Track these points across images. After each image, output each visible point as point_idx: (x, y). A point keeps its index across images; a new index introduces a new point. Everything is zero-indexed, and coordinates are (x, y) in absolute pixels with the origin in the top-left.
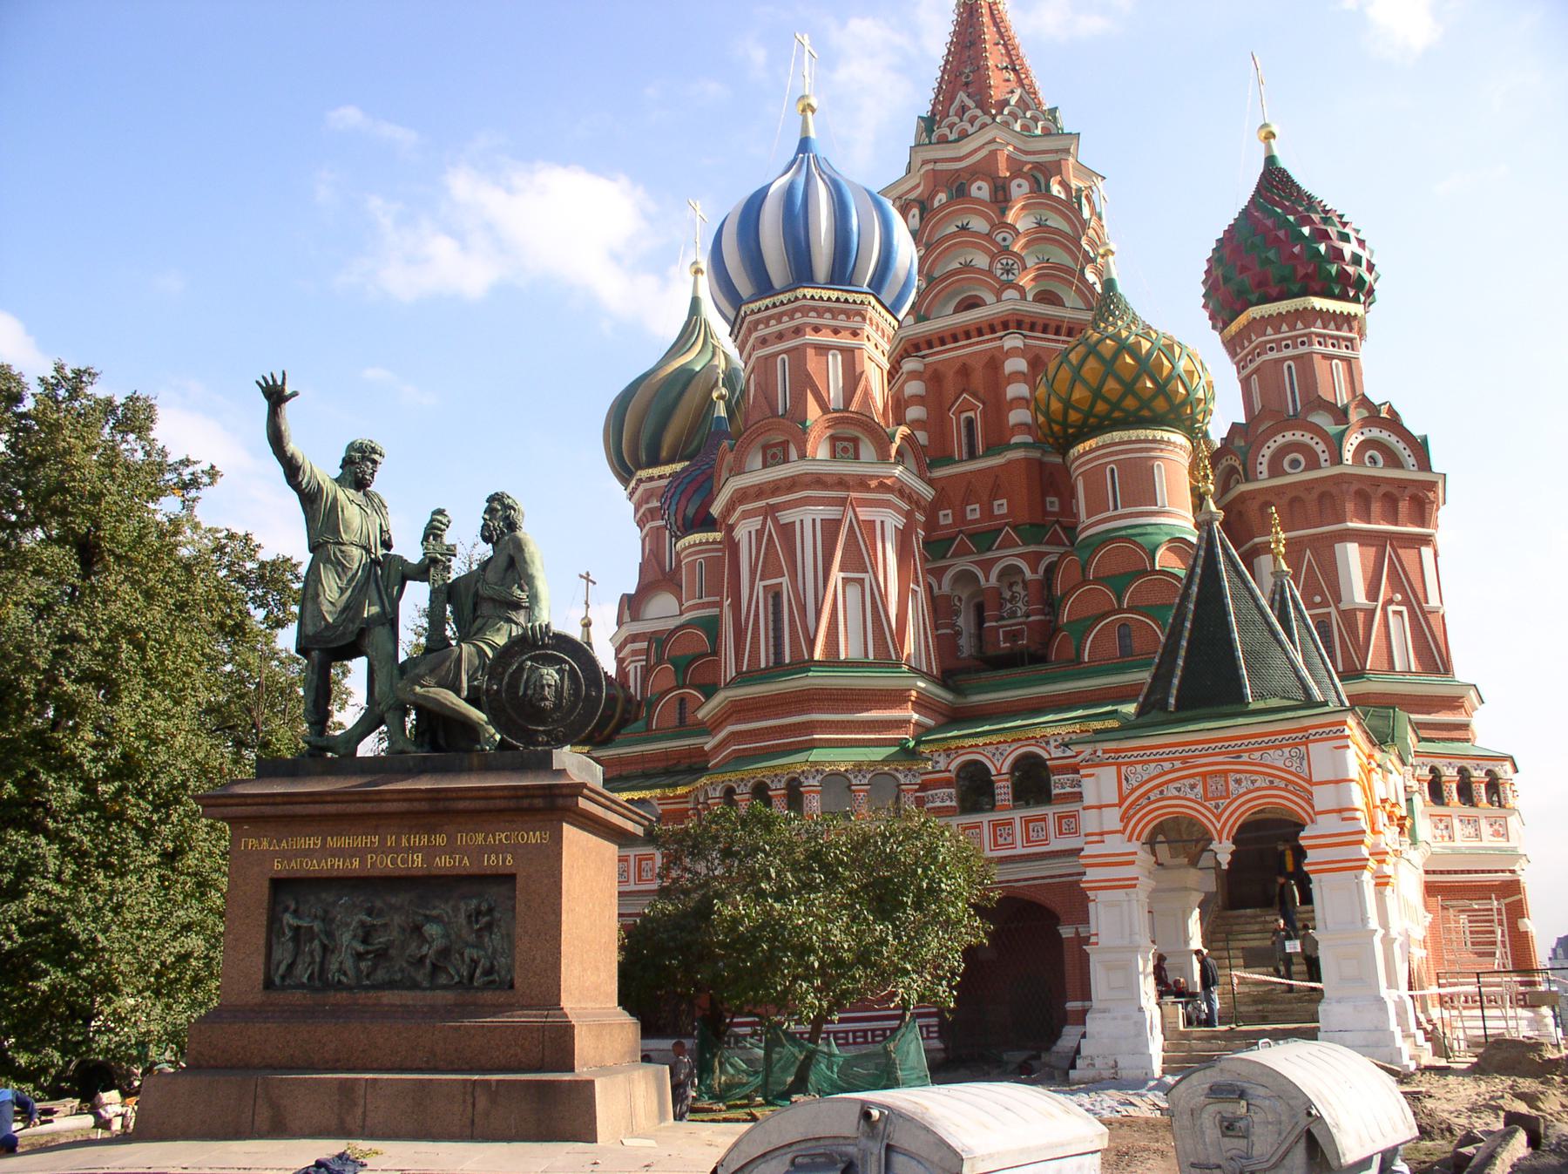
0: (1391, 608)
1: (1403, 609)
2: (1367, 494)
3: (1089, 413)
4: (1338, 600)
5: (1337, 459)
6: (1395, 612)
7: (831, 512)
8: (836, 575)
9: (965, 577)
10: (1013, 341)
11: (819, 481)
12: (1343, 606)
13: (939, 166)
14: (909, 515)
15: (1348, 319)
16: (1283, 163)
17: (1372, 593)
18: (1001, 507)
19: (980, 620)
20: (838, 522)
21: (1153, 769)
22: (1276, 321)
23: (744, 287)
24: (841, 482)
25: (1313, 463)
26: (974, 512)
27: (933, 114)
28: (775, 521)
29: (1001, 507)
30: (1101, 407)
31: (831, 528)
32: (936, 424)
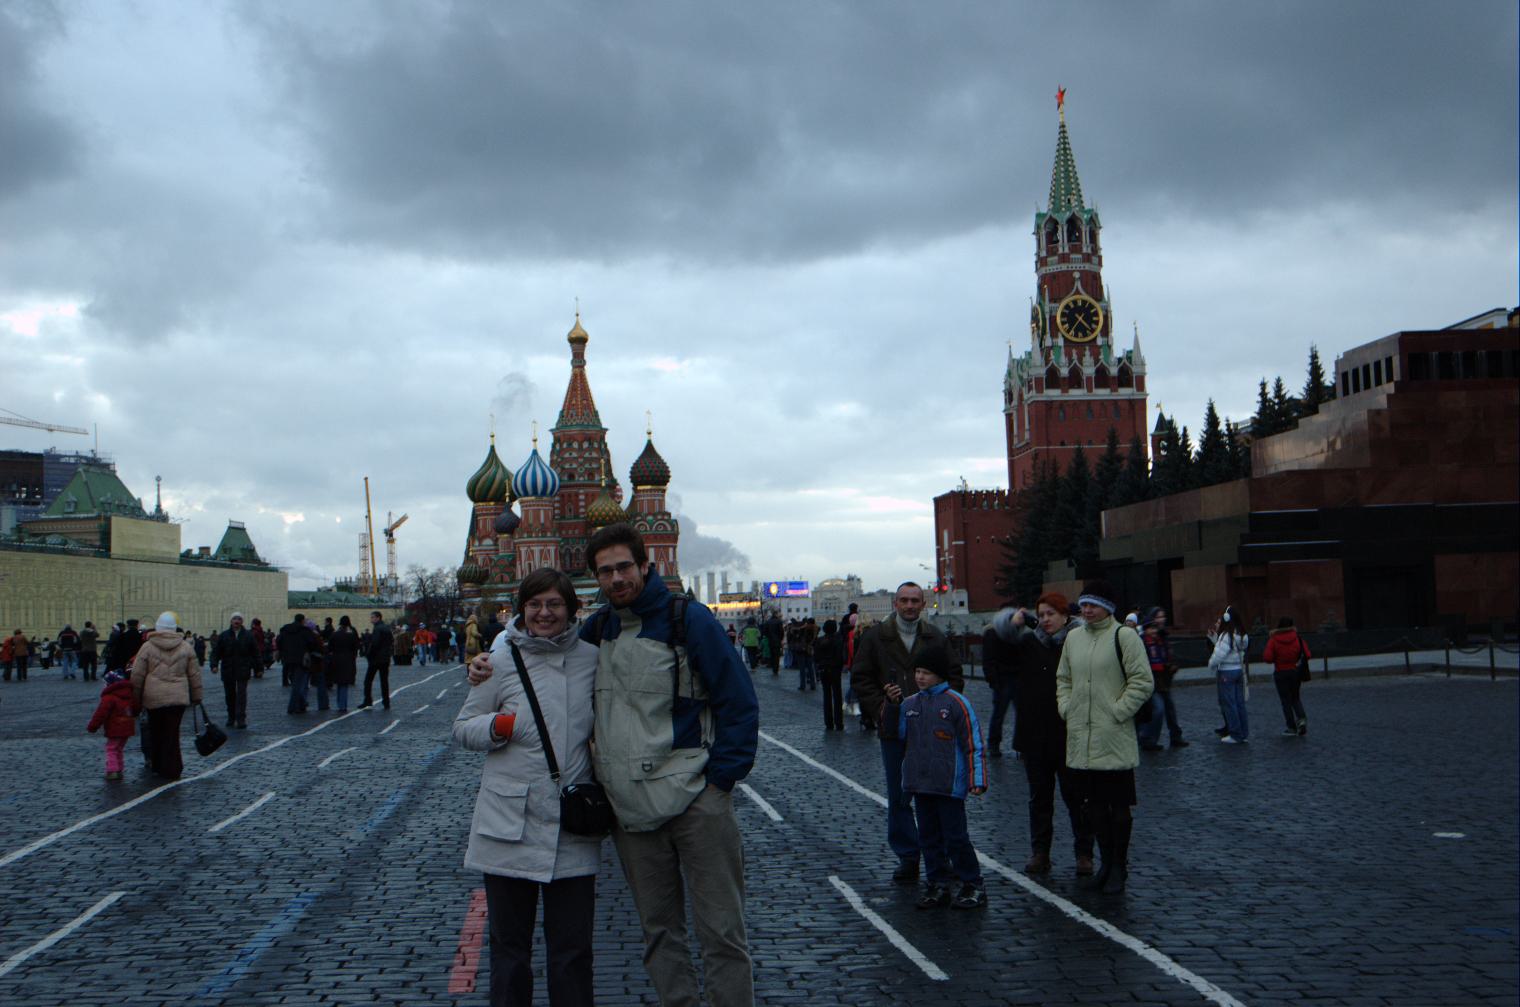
2: (657, 537)
5: (651, 528)
9: (567, 549)
10: (581, 491)
11: (538, 542)
15: (658, 490)
16: (653, 442)
17: (656, 558)
18: (577, 532)
19: (571, 560)
22: (644, 490)
23: (521, 492)
24: (543, 542)
26: (570, 532)
27: (563, 410)
29: (577, 532)
31: (541, 552)
32: (562, 508)
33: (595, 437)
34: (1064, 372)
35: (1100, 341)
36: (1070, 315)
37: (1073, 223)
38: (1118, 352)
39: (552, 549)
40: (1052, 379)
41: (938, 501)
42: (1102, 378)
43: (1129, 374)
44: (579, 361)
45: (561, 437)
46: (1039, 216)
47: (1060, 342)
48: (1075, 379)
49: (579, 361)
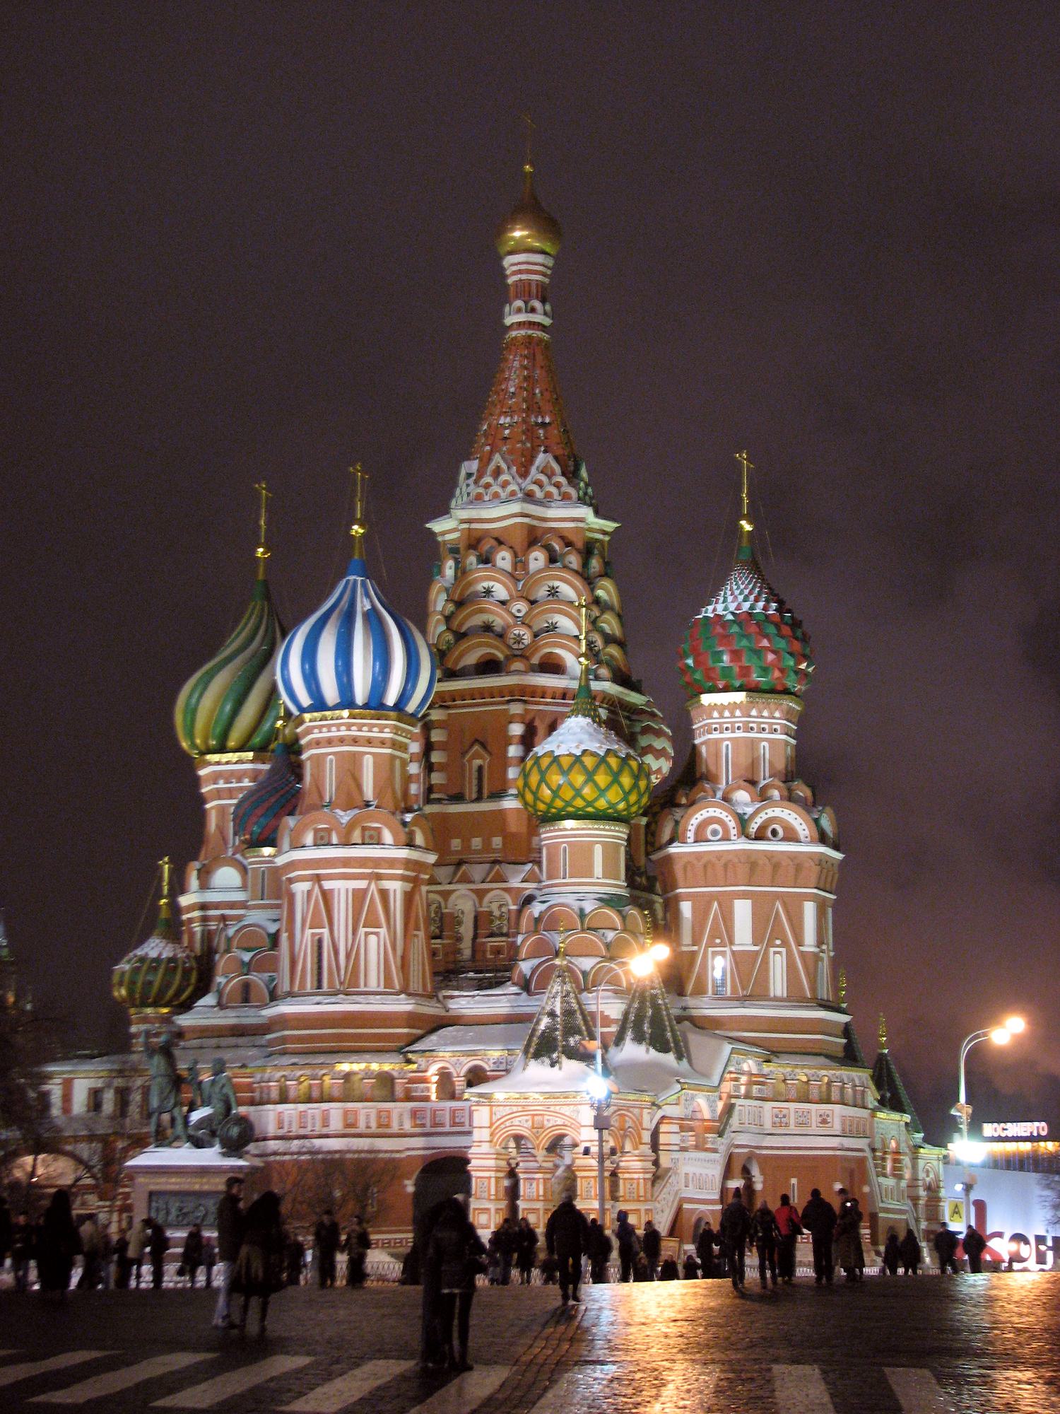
0: (772, 950)
1: (783, 950)
3: (550, 805)
4: (732, 943)
6: (775, 953)
7: (362, 884)
8: (362, 931)
10: (516, 709)
12: (735, 948)
13: (474, 526)
14: (415, 881)
20: (365, 891)
21: (508, 1110)
25: (726, 838)
28: (321, 887)
30: (559, 804)
31: (359, 896)
39: (396, 888)
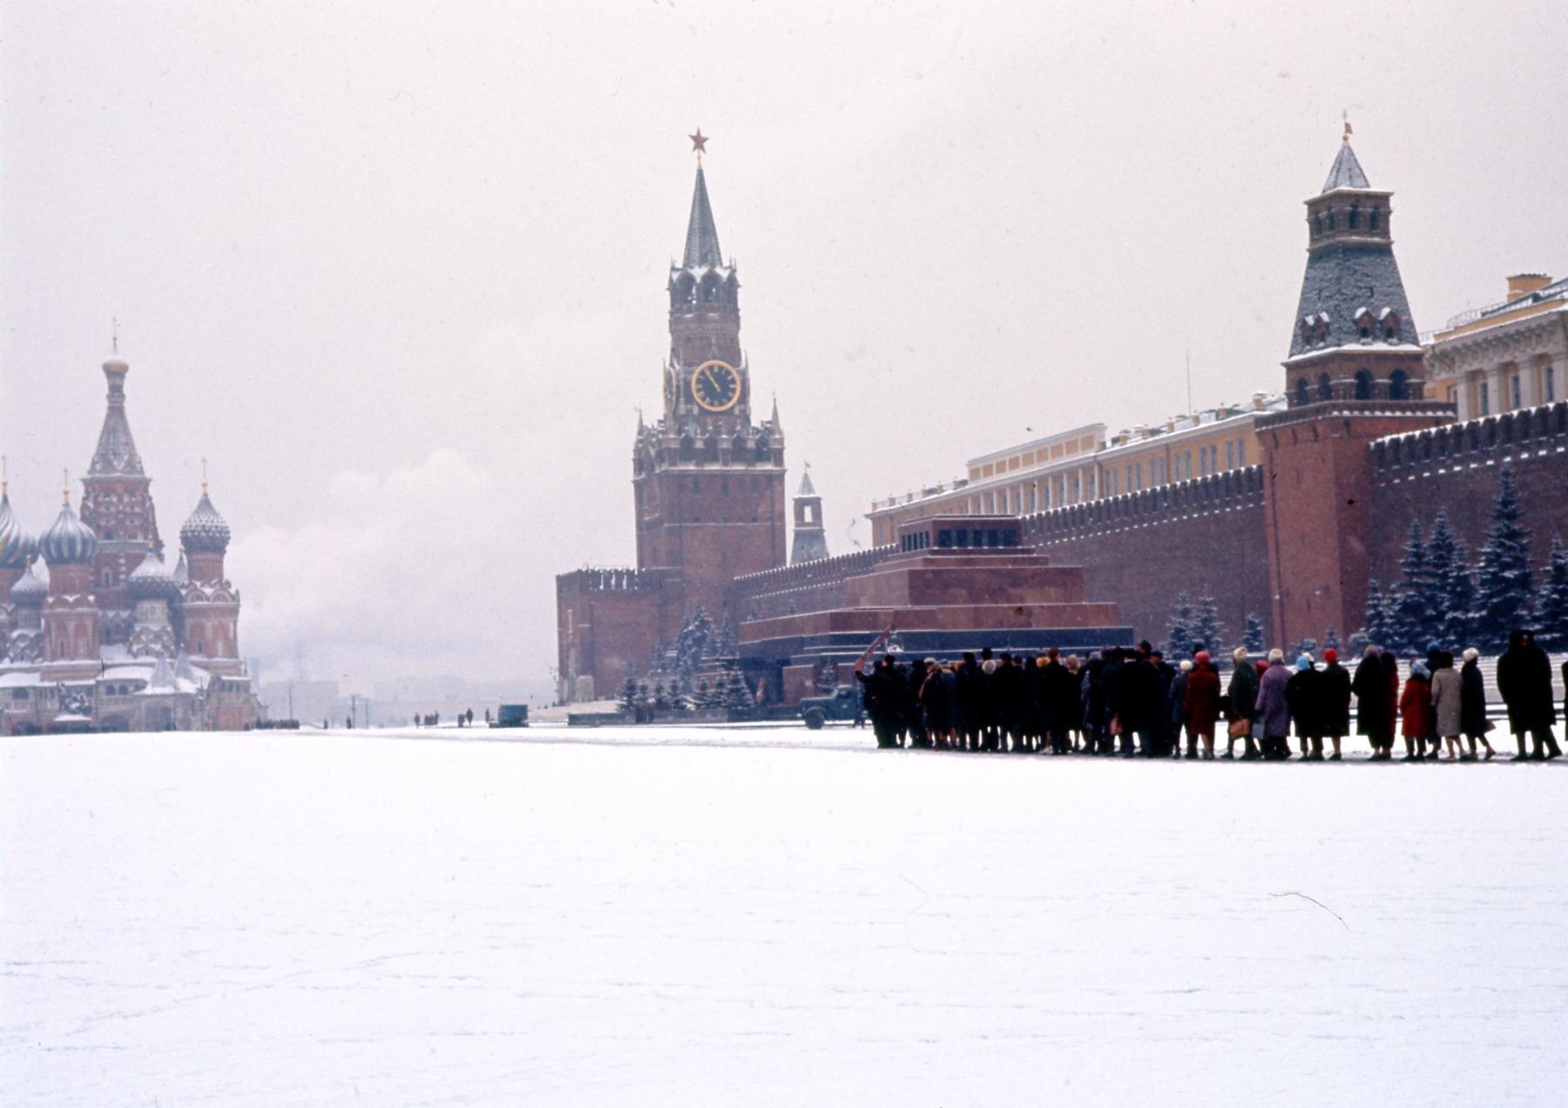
33: (139, 488)
34: (699, 445)
35: (737, 411)
36: (704, 382)
37: (711, 278)
38: (755, 422)
40: (686, 451)
41: (559, 578)
42: (739, 451)
43: (768, 447)
44: (116, 392)
45: (95, 487)
46: (673, 269)
47: (696, 411)
48: (711, 453)
49: (116, 392)
